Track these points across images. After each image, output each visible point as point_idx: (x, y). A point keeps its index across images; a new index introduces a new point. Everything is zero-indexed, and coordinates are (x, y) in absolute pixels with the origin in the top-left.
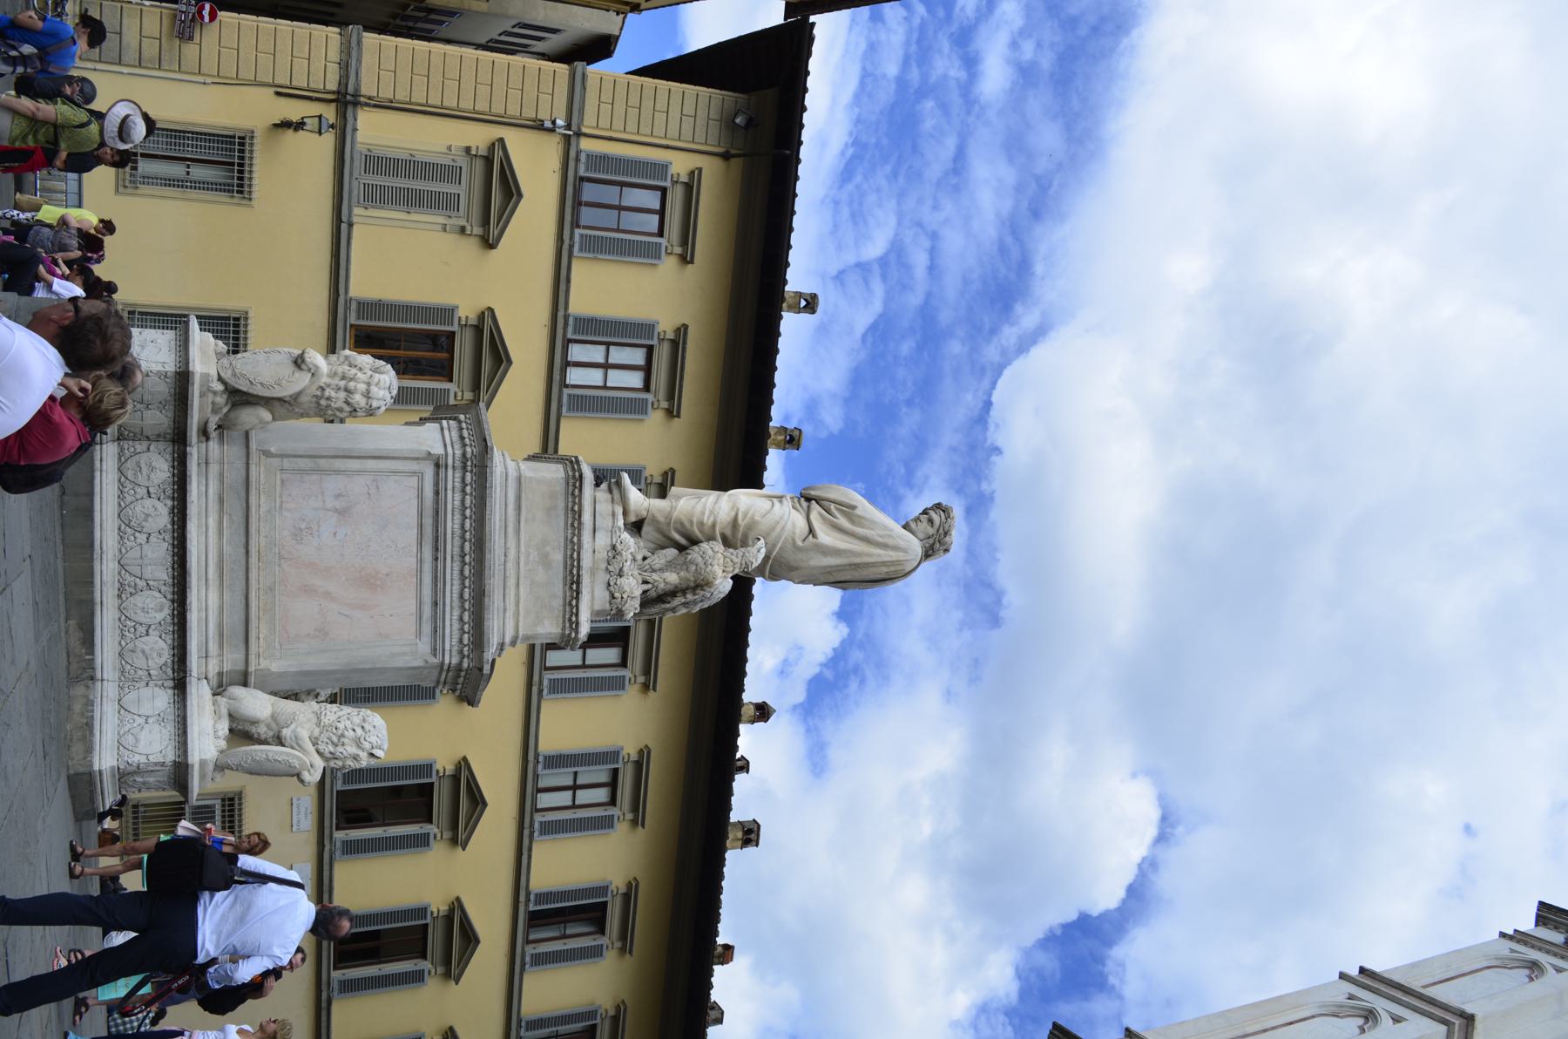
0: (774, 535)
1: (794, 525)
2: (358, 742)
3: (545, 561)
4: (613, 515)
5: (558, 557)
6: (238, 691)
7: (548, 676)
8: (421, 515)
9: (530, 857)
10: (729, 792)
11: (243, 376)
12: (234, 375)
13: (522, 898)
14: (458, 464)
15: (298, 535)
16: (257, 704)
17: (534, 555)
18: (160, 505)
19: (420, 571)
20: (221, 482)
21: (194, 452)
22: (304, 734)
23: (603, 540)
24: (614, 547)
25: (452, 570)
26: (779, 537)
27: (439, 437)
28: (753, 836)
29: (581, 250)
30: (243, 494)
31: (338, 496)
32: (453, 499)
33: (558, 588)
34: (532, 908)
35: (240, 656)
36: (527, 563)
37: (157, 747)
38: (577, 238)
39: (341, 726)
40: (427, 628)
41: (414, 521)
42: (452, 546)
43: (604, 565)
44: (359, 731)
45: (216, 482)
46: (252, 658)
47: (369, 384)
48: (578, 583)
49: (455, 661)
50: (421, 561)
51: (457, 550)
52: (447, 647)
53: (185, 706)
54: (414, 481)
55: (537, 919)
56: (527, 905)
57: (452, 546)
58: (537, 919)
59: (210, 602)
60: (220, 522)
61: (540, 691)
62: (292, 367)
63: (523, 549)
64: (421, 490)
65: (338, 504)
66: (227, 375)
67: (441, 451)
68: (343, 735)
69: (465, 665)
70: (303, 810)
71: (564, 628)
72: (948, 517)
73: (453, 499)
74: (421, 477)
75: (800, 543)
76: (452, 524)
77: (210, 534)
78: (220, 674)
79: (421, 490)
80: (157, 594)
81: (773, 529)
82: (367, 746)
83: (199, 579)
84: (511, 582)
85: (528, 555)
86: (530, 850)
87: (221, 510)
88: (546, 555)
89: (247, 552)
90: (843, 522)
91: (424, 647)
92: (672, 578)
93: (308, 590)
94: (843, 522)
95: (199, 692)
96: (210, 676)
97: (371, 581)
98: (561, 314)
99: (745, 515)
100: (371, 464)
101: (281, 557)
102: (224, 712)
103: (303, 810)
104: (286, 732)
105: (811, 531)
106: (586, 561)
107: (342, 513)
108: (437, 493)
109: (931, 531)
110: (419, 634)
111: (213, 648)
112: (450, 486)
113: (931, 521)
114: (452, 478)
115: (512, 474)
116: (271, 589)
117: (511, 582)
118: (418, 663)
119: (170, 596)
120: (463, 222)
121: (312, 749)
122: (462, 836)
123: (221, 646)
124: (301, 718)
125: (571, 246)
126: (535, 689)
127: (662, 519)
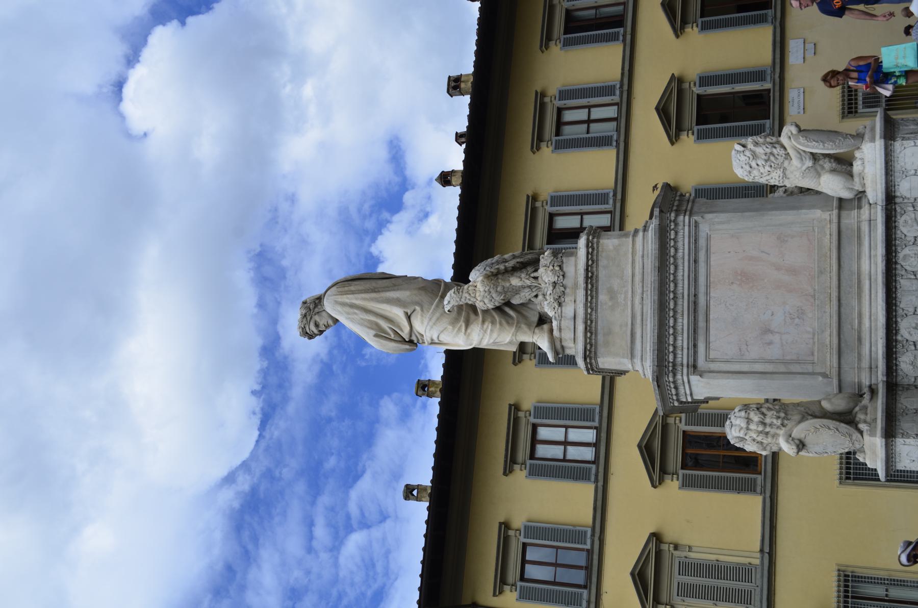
0: (438, 314)
1: (422, 323)
2: (755, 156)
3: (612, 294)
4: (560, 330)
5: (603, 297)
6: (846, 195)
7: (609, 207)
8: (707, 329)
9: (623, 69)
10: (471, 118)
11: (843, 435)
12: (850, 435)
13: (629, 37)
14: (679, 368)
15: (801, 313)
16: (831, 184)
17: (621, 298)
18: (907, 336)
19: (707, 286)
20: (859, 354)
21: (880, 376)
22: (795, 162)
23: (568, 310)
24: (560, 305)
25: (683, 287)
26: (433, 313)
27: (693, 388)
28: (453, 84)
29: (586, 532)
30: (843, 345)
31: (770, 343)
32: (683, 341)
33: (602, 274)
34: (621, 30)
35: (844, 221)
36: (626, 292)
37: (908, 152)
38: (589, 541)
39: (767, 168)
40: (702, 242)
41: (712, 325)
42: (684, 305)
43: (568, 291)
44: (754, 164)
45: (863, 353)
46: (835, 220)
47: (748, 429)
48: (587, 277)
49: (681, 218)
50: (707, 294)
51: (680, 302)
52: (686, 228)
53: (887, 183)
54: (712, 355)
55: (617, 21)
56: (625, 32)
57: (684, 305)
58: (617, 21)
59: (867, 262)
60: (860, 323)
61: (615, 195)
62: (807, 441)
63: (629, 303)
64: (707, 348)
65: (769, 337)
66: (856, 435)
67: (692, 378)
68: (766, 161)
69: (673, 215)
70: (796, 105)
71: (598, 243)
72: (303, 329)
73: (683, 341)
74: (708, 359)
75: (418, 308)
76: (683, 322)
77: (867, 314)
78: (860, 207)
79: (707, 348)
80: (908, 268)
81: (438, 319)
82: (748, 153)
83: (876, 280)
84: (638, 278)
85: (625, 298)
86: (623, 74)
87: (860, 332)
88: (611, 298)
89: (839, 300)
90: (384, 325)
91: (704, 229)
92: (515, 281)
93: (793, 271)
94: (384, 325)
95: (875, 192)
96: (867, 206)
97: (745, 278)
98: (601, 484)
99: (459, 329)
100: (745, 368)
101: (814, 296)
102: (856, 179)
103: (796, 105)
104: (809, 163)
105: (409, 318)
106: (581, 294)
107: (767, 331)
108: (695, 346)
109: (317, 318)
110: (708, 239)
111: (865, 227)
112: (685, 351)
113: (317, 325)
114: (683, 357)
115: (637, 361)
116: (821, 272)
117: (638, 278)
118: (708, 216)
119: (898, 266)
120: (676, 553)
121: (790, 150)
122: (675, 85)
123: (859, 229)
124: (798, 174)
125: (593, 535)
126: (619, 196)
127: (523, 326)
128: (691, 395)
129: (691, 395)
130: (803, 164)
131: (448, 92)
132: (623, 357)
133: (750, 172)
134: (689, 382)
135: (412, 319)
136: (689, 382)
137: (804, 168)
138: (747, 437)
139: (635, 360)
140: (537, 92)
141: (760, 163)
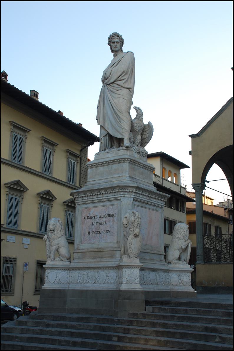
8: (141, 207)
9: (32, 169)
13: (40, 174)
18: (145, 274)
22: (184, 244)
24: (138, 153)
25: (153, 200)
27: (127, 198)
39: (183, 234)
40: (158, 209)
52: (163, 205)
70: (11, 238)
73: (141, 197)
76: (145, 198)
102: (176, 261)
103: (11, 238)
105: (128, 88)
109: (119, 44)
113: (117, 42)
128: (124, 197)
129: (124, 197)
130: (183, 245)
131: (34, 90)
132: (129, 173)
133: (182, 228)
134: (131, 197)
135: (128, 90)
136: (131, 197)
137: (182, 245)
138: (136, 217)
139: (128, 178)
140: (30, 130)
141: (185, 232)
